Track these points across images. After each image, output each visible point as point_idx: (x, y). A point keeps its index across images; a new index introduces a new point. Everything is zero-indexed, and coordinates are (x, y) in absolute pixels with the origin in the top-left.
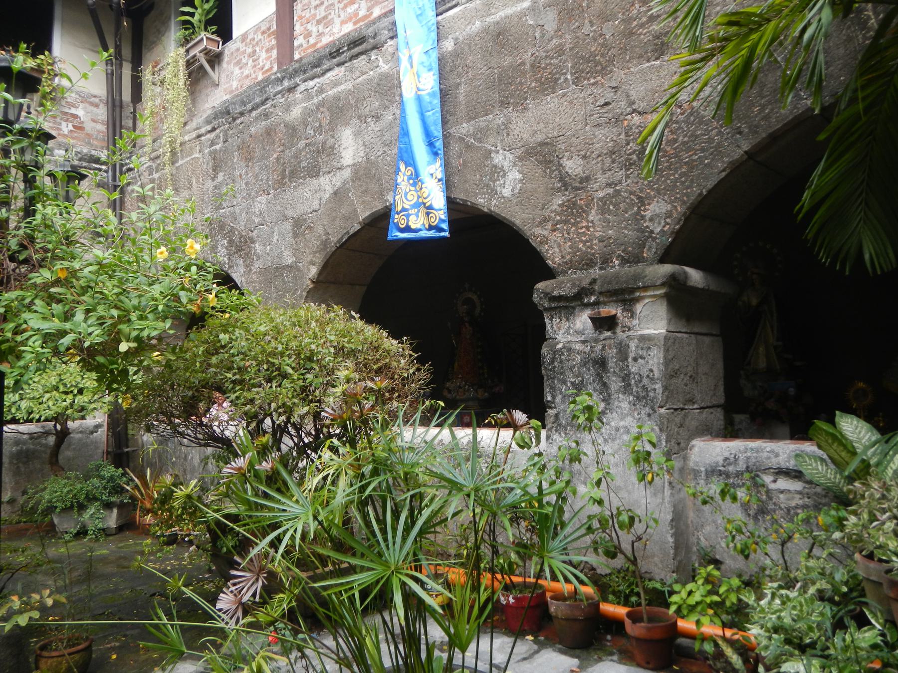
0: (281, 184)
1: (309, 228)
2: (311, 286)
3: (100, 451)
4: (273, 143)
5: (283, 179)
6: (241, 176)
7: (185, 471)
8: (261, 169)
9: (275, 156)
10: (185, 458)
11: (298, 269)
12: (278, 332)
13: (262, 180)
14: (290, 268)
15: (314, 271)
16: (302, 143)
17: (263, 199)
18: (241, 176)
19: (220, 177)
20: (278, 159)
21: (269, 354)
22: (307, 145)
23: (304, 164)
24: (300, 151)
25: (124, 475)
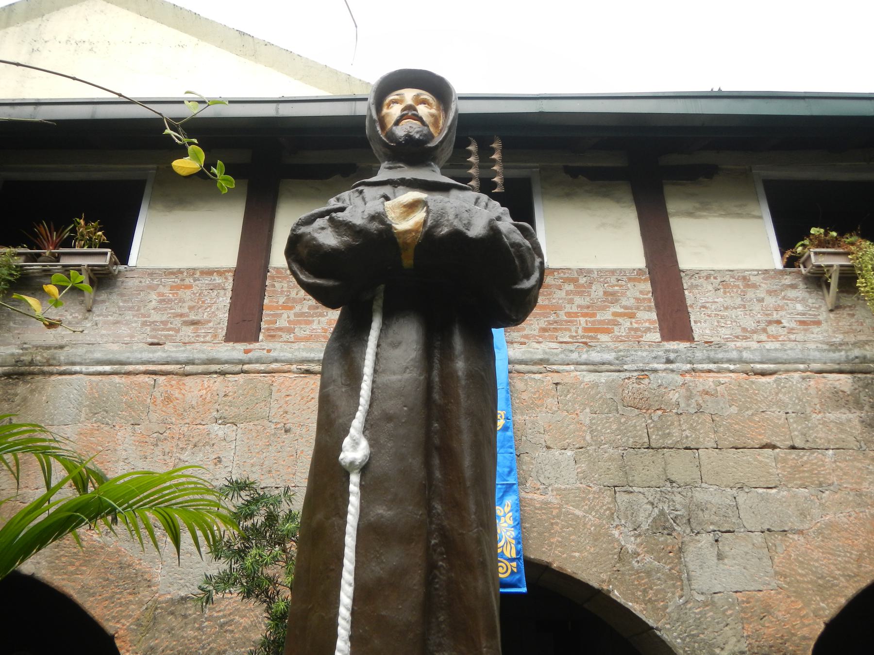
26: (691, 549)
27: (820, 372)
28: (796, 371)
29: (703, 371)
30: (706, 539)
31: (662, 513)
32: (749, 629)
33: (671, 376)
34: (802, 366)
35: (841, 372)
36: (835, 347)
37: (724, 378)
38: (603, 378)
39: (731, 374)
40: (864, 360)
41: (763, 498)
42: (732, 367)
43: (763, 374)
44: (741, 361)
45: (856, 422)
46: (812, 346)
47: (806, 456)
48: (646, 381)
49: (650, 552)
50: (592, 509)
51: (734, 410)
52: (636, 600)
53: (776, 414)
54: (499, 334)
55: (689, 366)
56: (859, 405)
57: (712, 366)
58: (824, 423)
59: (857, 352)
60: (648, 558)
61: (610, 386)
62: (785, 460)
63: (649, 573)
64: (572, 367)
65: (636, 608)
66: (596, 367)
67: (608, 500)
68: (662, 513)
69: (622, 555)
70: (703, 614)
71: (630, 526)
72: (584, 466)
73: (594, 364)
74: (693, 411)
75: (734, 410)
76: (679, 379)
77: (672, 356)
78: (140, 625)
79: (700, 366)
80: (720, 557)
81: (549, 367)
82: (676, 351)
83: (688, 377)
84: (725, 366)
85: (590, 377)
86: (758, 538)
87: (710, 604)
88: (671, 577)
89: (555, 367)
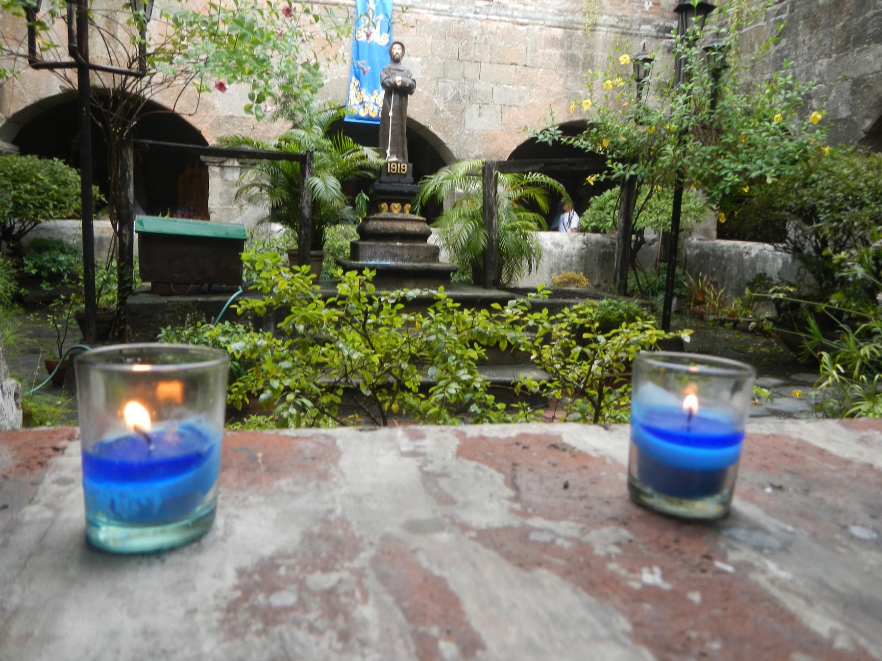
0: (844, 49)
1: (868, 87)
2: (864, 136)
3: (654, 259)
4: (841, 12)
5: (846, 45)
6: (804, 41)
7: (723, 279)
8: (826, 35)
9: (841, 24)
10: (725, 269)
11: (852, 121)
12: (857, 174)
13: (825, 45)
14: (844, 121)
15: (868, 123)
16: (870, 13)
17: (824, 62)
18: (804, 41)
19: (784, 42)
20: (844, 27)
21: (853, 189)
22: (875, 15)
23: (870, 31)
24: (867, 20)
25: (684, 274)
26: (468, 111)
27: (550, 26)
28: (538, 24)
29: (492, 20)
30: (475, 107)
31: (458, 93)
32: (485, 146)
33: (475, 21)
34: (541, 22)
35: (559, 27)
36: (561, 12)
37: (502, 25)
38: (441, 19)
39: (506, 24)
40: (572, 22)
41: (505, 89)
42: (507, 19)
43: (522, 24)
44: (512, 16)
45: (558, 56)
46: (550, 10)
47: (530, 70)
48: (462, 23)
49: (450, 110)
50: (425, 88)
51: (502, 43)
52: (440, 131)
53: (522, 47)
54: (409, 96)
55: (485, 17)
56: (562, 46)
57: (497, 18)
58: (543, 55)
59: (570, 17)
60: (448, 113)
61: (444, 24)
62: (520, 72)
63: (447, 120)
64: (426, 11)
65: (439, 134)
66: (438, 13)
67: (434, 84)
68: (458, 93)
69: (437, 111)
70: (467, 139)
71: (442, 98)
72: (425, 67)
73: (437, 10)
74: (482, 42)
75: (502, 43)
76: (479, 24)
77: (478, 10)
78: (212, 127)
79: (490, 17)
80: (480, 115)
81: (414, 10)
82: (481, 8)
83: (484, 23)
84: (504, 18)
85: (434, 18)
86: (498, 108)
87: (471, 135)
88: (456, 122)
89: (417, 10)
